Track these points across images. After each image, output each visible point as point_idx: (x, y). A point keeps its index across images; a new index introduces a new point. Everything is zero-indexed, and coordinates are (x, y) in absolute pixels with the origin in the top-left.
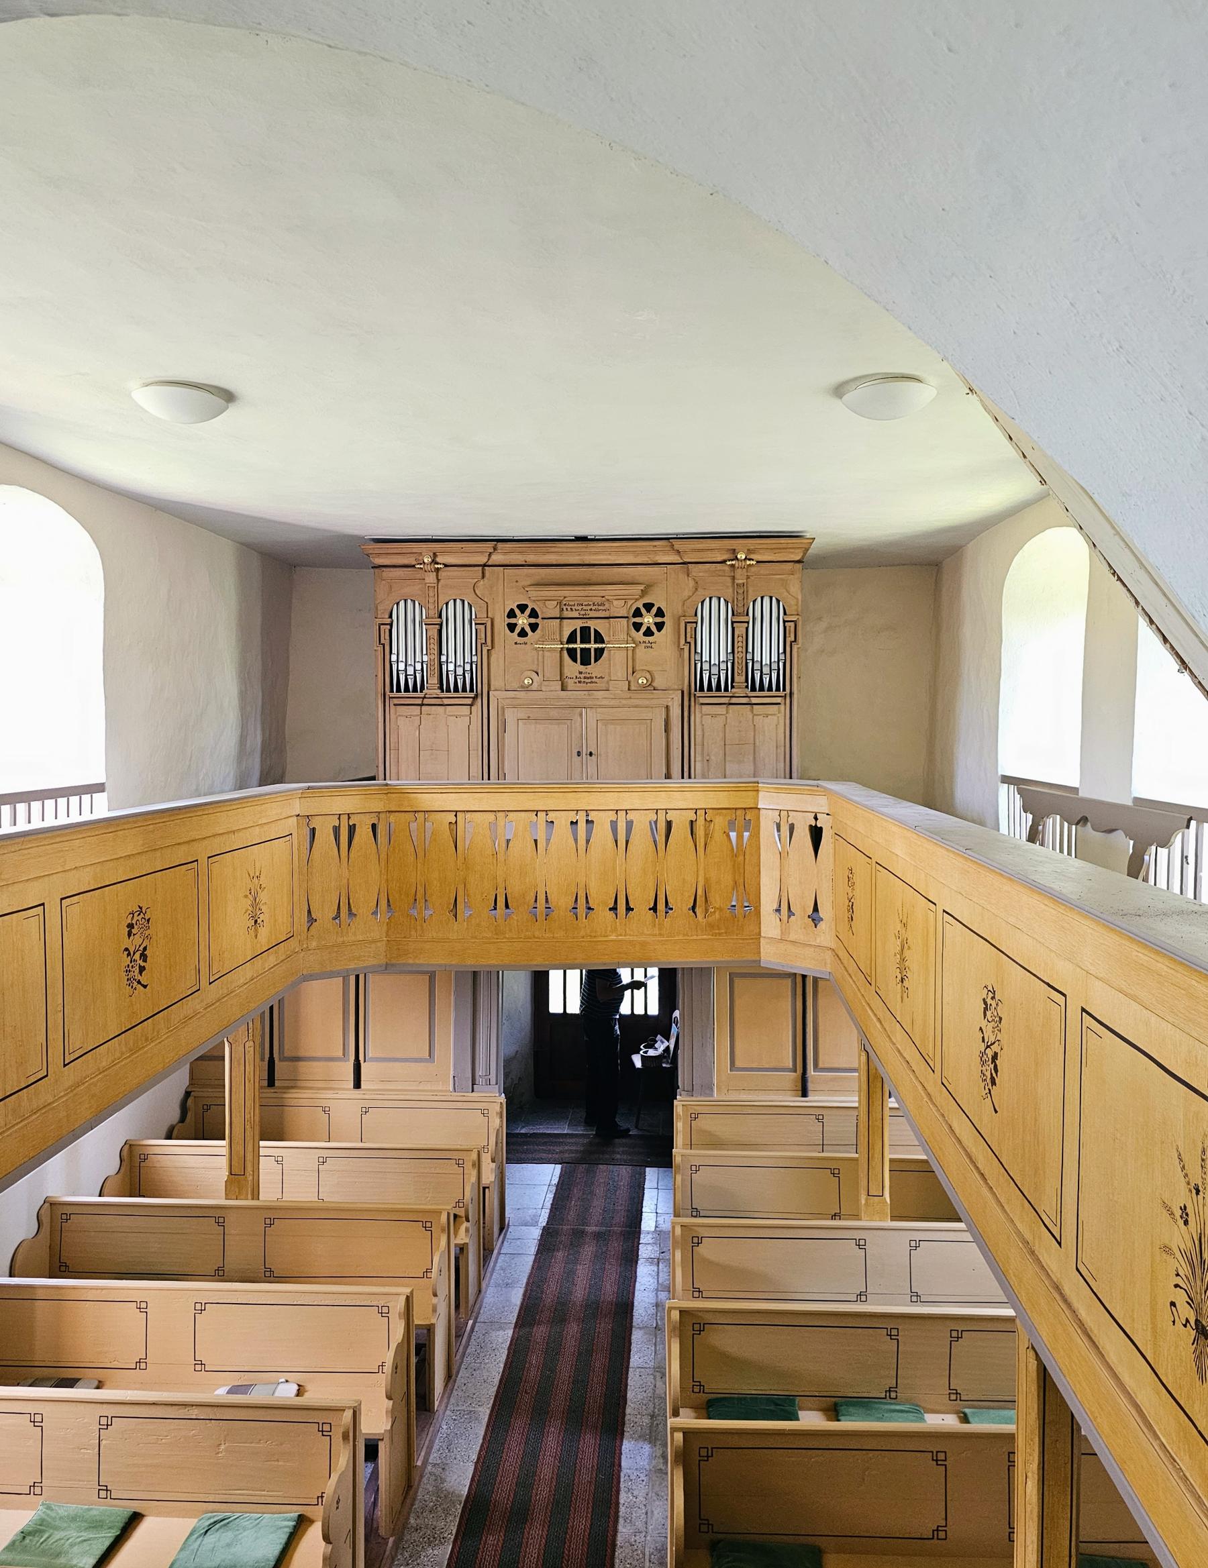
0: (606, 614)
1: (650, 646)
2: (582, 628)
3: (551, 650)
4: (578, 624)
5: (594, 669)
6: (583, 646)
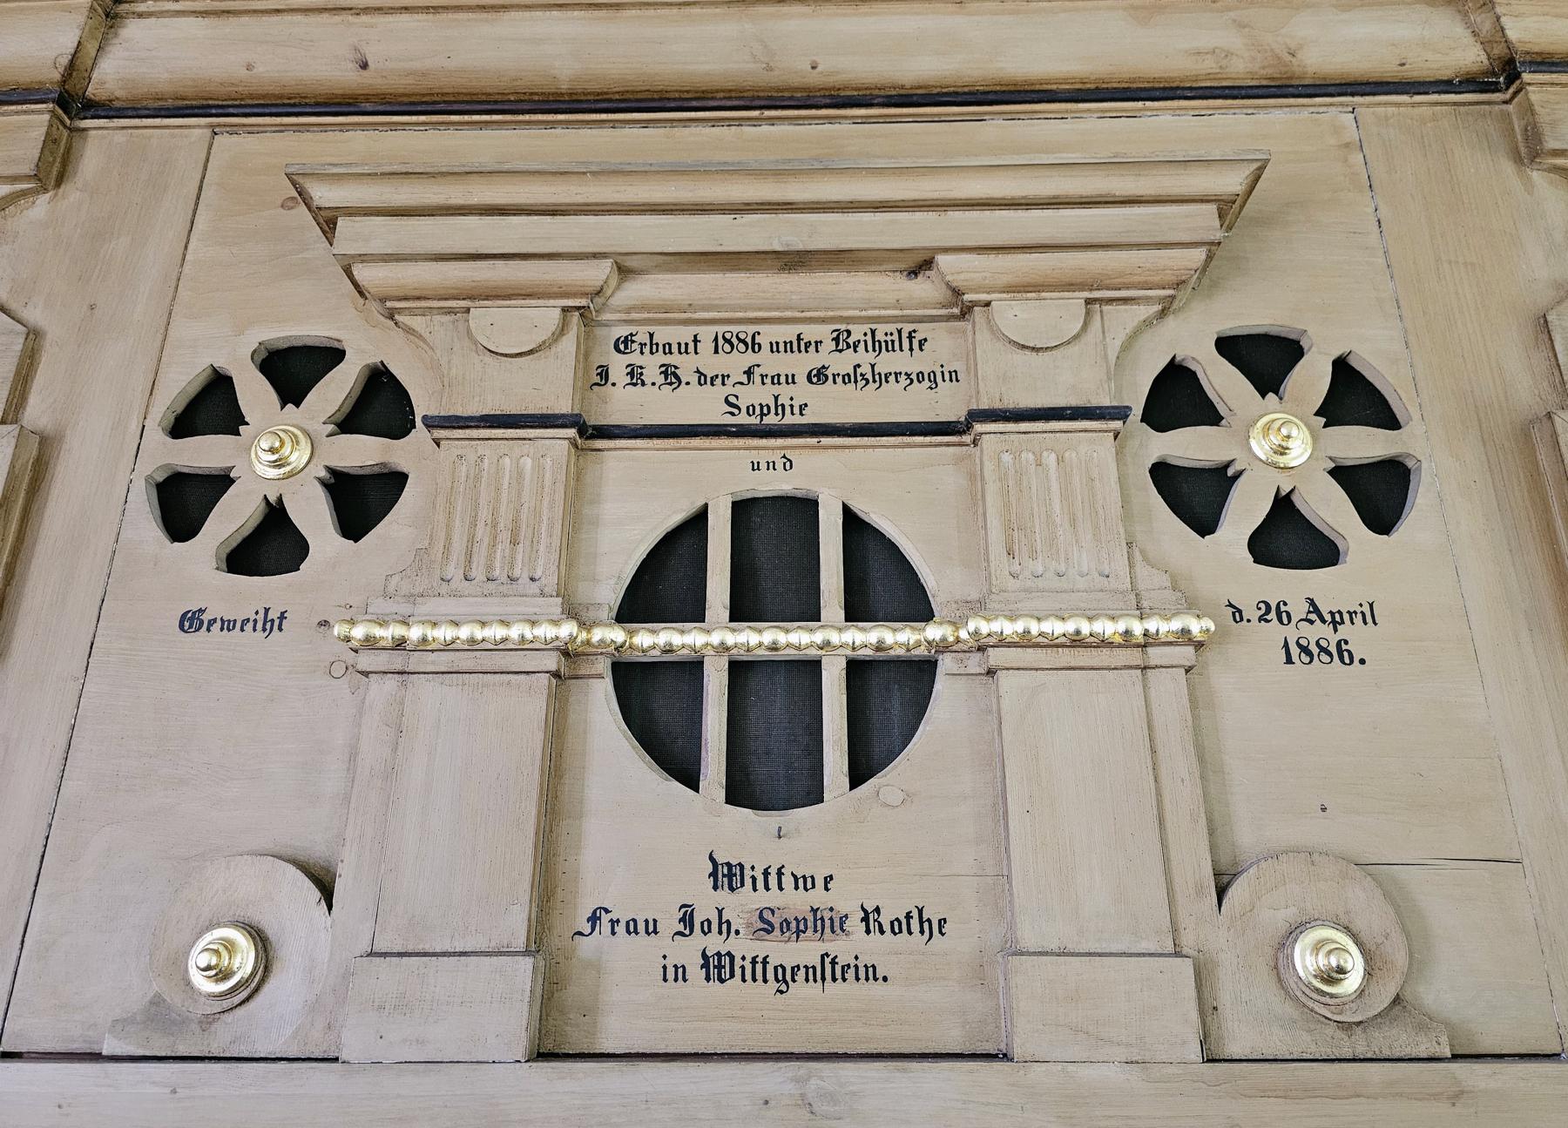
0: (947, 404)
1: (1327, 644)
2: (743, 510)
3: (476, 664)
4: (721, 478)
5: (844, 838)
6: (756, 639)
